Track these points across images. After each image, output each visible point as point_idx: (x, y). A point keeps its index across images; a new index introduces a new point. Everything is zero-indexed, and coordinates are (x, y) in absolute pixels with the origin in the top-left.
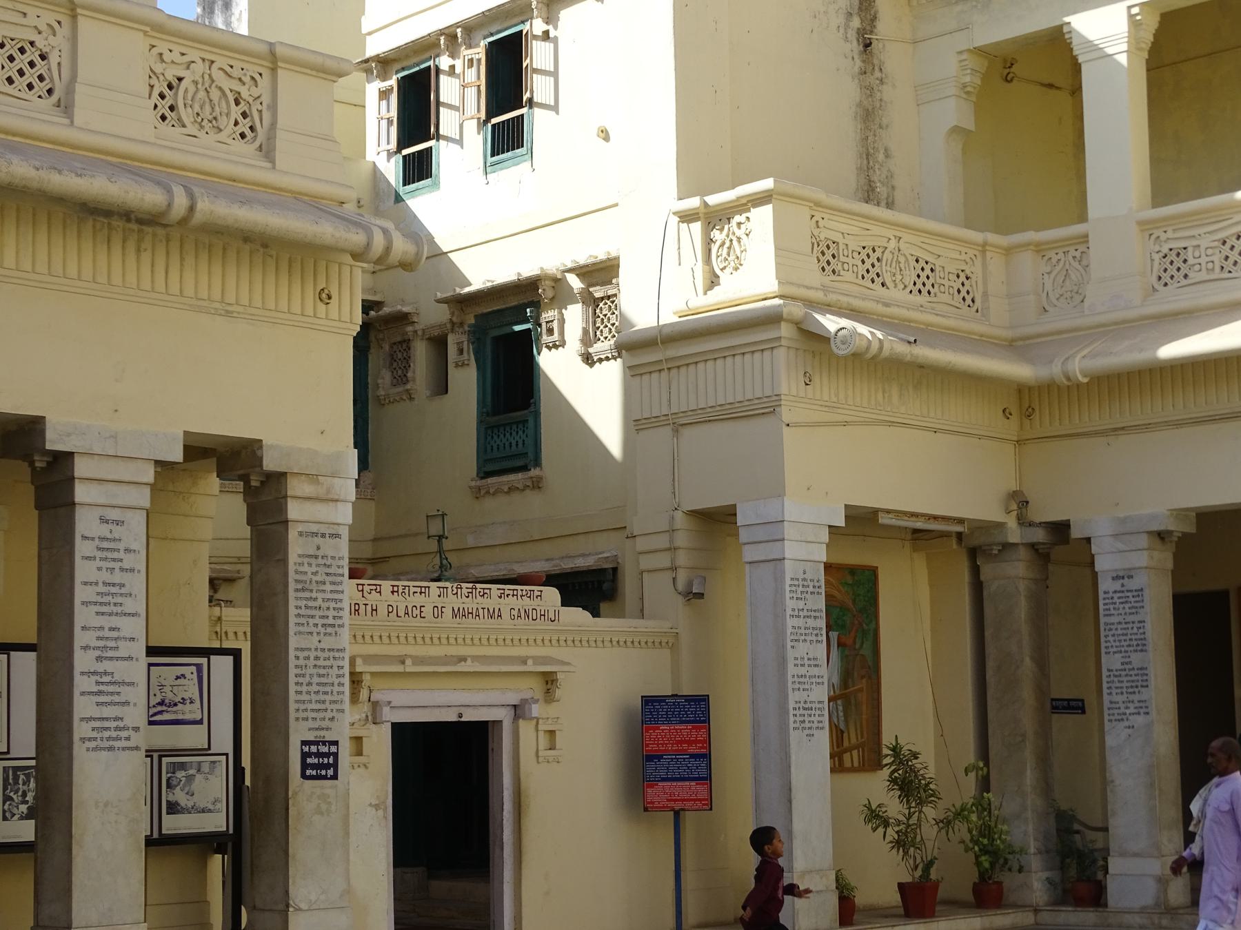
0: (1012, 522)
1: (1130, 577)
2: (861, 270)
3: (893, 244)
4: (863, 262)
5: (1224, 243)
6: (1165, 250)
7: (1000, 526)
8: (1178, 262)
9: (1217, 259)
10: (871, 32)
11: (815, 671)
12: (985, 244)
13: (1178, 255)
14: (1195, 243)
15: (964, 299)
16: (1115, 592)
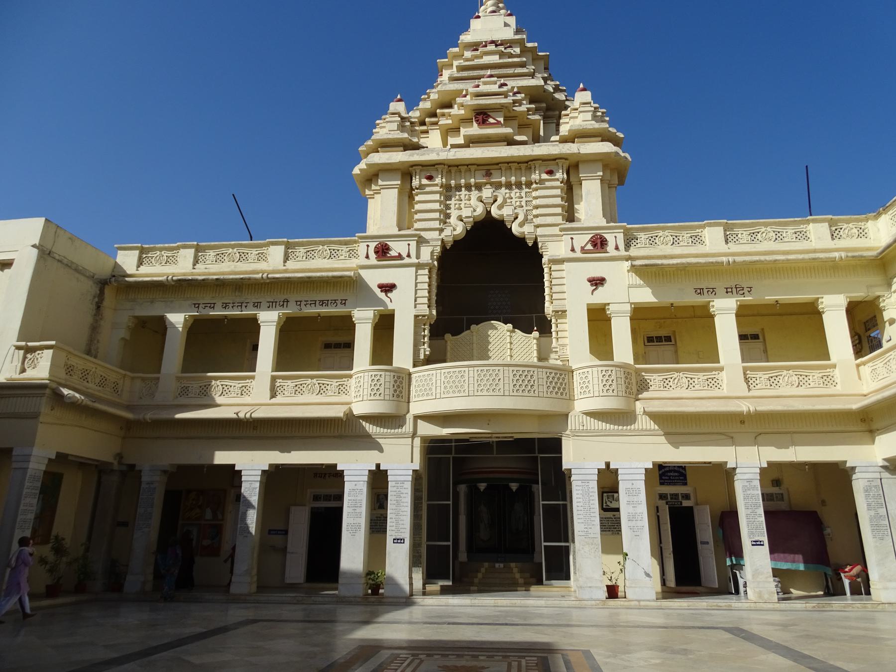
0: (116, 463)
1: (152, 484)
2: (81, 376)
3: (94, 370)
4: (82, 374)
5: (201, 387)
6: (182, 386)
7: (111, 464)
8: (186, 391)
9: (198, 391)
10: (101, 304)
11: (31, 508)
12: (125, 375)
13: (186, 388)
14: (192, 386)
15: (115, 390)
16: (146, 488)
